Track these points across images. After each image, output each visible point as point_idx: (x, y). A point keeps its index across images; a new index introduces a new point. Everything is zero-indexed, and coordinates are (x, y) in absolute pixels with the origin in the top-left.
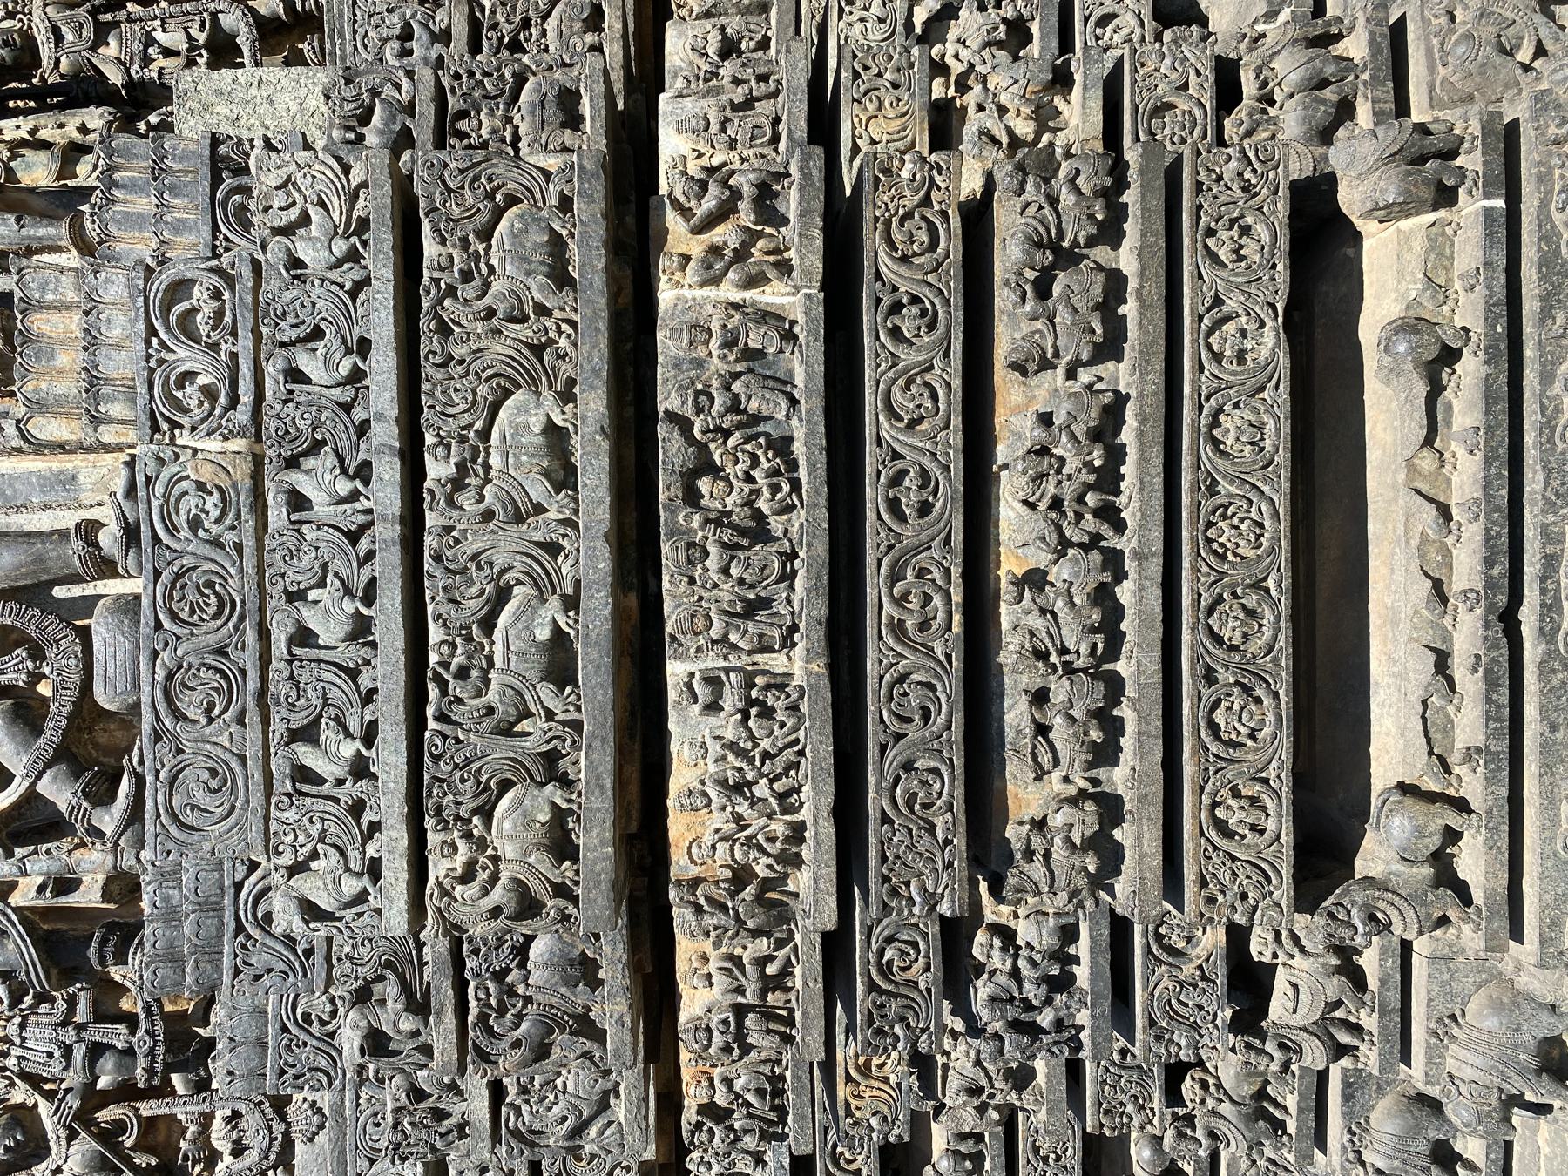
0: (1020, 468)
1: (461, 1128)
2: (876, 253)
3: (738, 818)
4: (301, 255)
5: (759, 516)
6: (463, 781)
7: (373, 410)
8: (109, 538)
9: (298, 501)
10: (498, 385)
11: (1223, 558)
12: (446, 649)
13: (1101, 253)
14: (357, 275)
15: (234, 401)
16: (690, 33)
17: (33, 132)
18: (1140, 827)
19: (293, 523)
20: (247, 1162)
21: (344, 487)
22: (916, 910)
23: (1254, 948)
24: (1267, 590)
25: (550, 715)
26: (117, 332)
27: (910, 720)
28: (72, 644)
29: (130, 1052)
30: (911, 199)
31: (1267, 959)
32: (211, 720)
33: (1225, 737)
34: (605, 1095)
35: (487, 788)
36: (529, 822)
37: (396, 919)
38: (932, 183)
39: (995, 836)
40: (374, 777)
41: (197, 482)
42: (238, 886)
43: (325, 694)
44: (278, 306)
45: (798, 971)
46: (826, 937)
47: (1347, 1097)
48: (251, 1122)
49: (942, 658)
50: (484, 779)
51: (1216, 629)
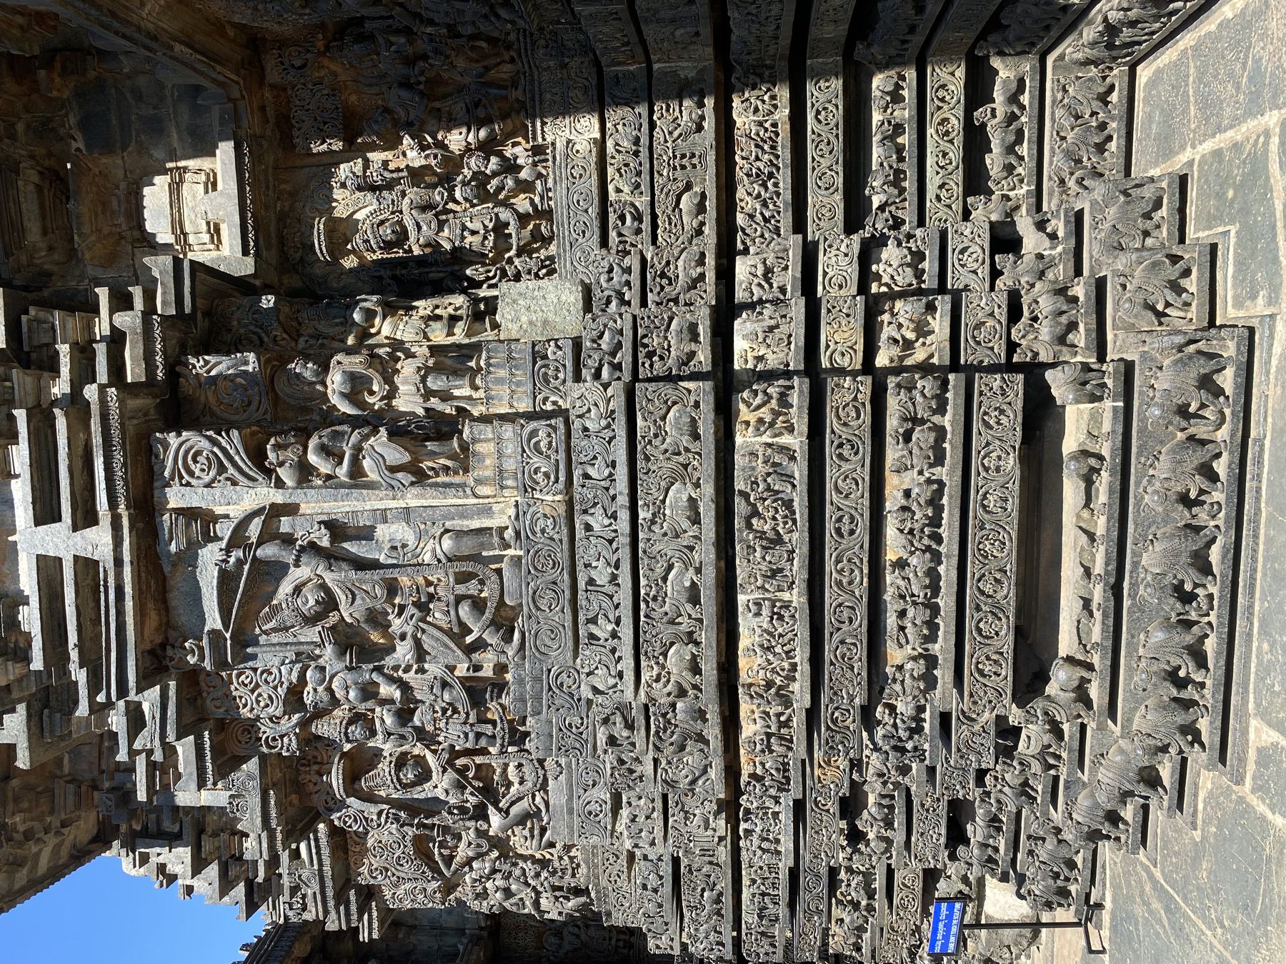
1: (641, 778)
3: (768, 660)
5: (778, 533)
9: (588, 527)
11: (986, 557)
13: (936, 419)
14: (611, 434)
15: (557, 481)
25: (690, 616)
28: (495, 578)
30: (849, 398)
34: (706, 766)
36: (683, 659)
37: (629, 694)
42: (549, 671)
47: (1066, 788)
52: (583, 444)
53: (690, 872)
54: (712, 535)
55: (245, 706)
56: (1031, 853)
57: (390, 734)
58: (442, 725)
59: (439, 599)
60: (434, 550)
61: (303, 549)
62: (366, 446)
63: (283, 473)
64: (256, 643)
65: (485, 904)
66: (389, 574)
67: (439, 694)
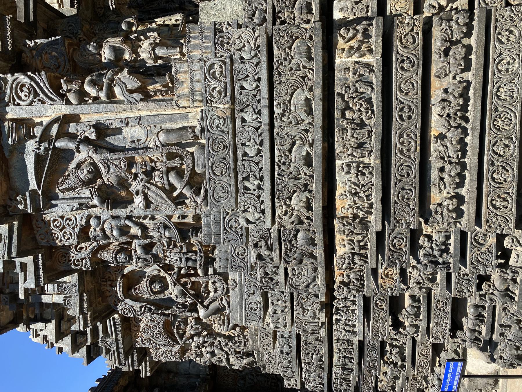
1: (277, 283)
3: (355, 201)
4: (243, 56)
5: (362, 120)
6: (284, 190)
8: (197, 130)
9: (244, 120)
11: (499, 130)
12: (280, 158)
13: (465, 41)
15: (226, 95)
17: (163, 22)
18: (469, 206)
20: (218, 294)
21: (255, 117)
22: (404, 227)
23: (505, 244)
24: (512, 139)
25: (306, 174)
26: (197, 78)
27: (404, 176)
28: (189, 156)
29: (195, 261)
30: (408, 29)
31: (509, 247)
32: (222, 175)
33: (497, 181)
34: (315, 277)
36: (300, 201)
37: (268, 223)
38: (414, 24)
39: (427, 208)
40: (262, 189)
42: (224, 218)
45: (369, 244)
46: (377, 233)
48: (219, 284)
49: (413, 159)
51: (495, 150)
52: (240, 67)
53: (306, 344)
54: (320, 121)
55: (57, 238)
56: (502, 335)
57: (139, 259)
58: (168, 254)
59: (158, 170)
60: (154, 141)
61: (81, 141)
62: (116, 78)
63: (71, 97)
64: (57, 198)
65: (202, 359)
66: (130, 155)
67: (162, 232)
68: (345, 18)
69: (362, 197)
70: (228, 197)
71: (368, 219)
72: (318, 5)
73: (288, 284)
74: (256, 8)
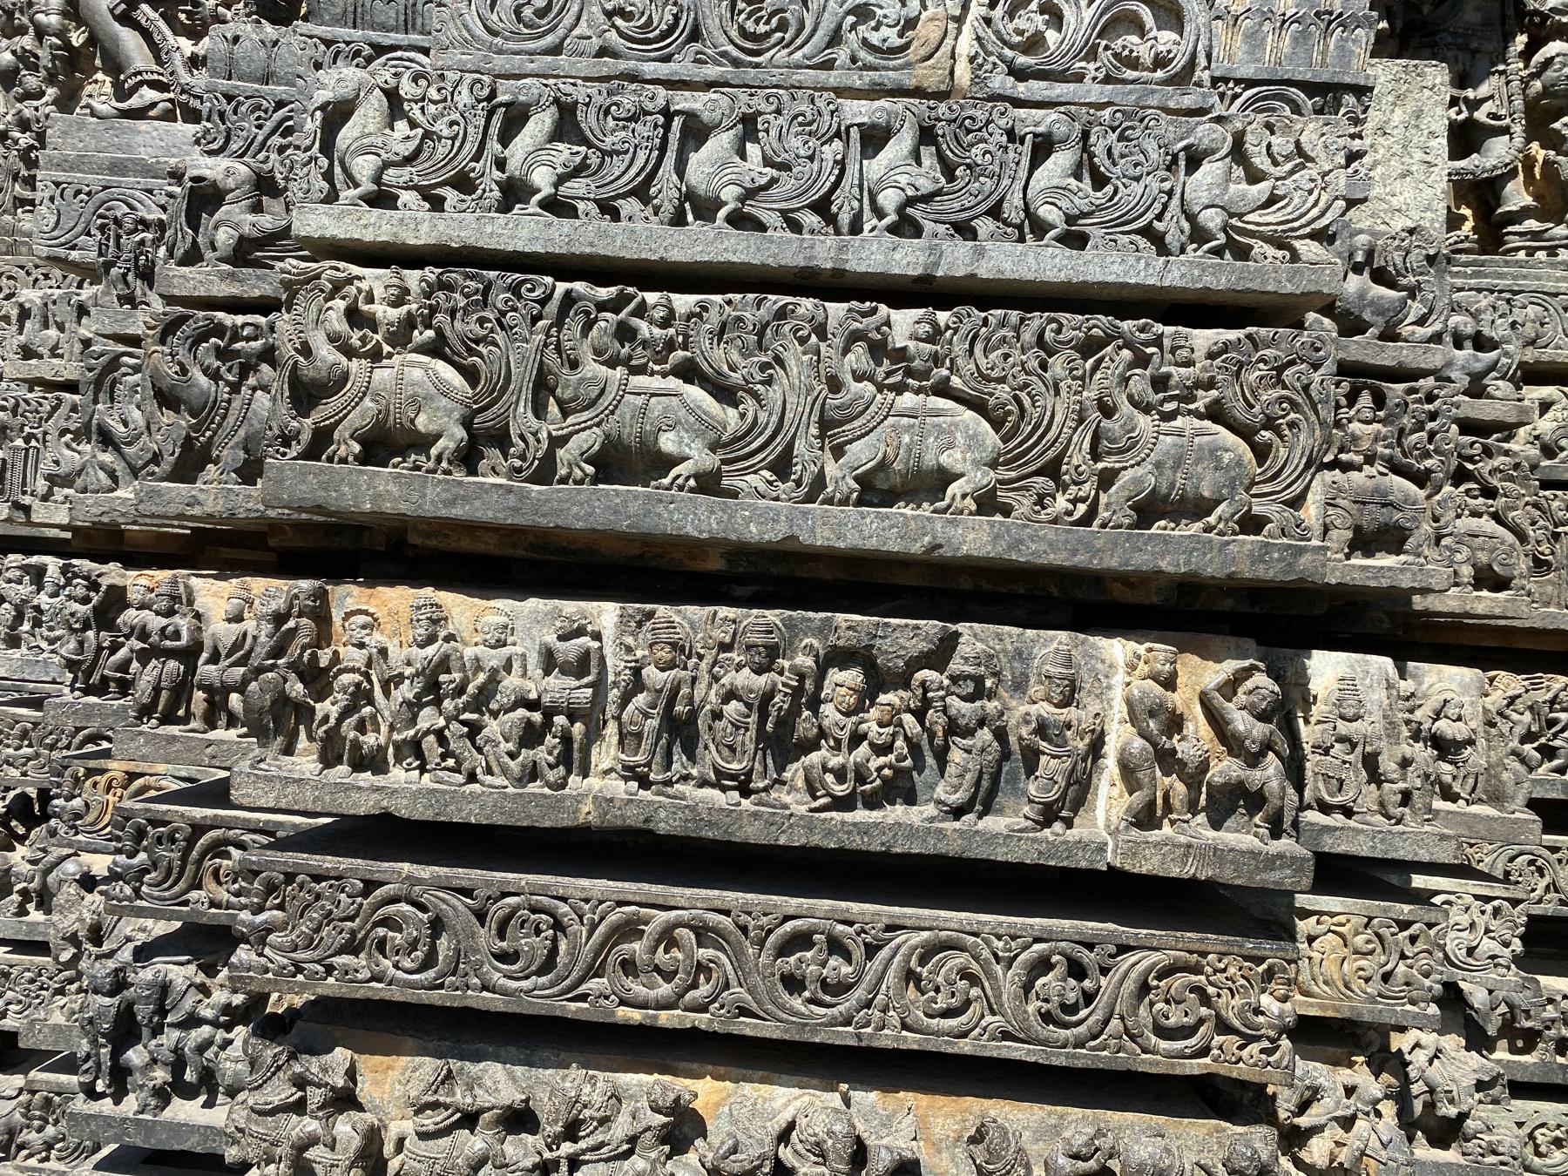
0: (837, 1128)
2: (1156, 949)
4: (1206, 167)
6: (482, 321)
7: (989, 245)
9: (874, 138)
10: (1009, 413)
12: (659, 314)
15: (1020, 74)
16: (1466, 699)
19: (848, 128)
25: (563, 440)
30: (1231, 1006)
32: (609, 15)
35: (469, 349)
36: (417, 404)
38: (1250, 1040)
40: (505, 207)
41: (917, 18)
43: (618, 153)
44: (1138, 132)
45: (232, 734)
50: (481, 348)
52: (1151, 146)
68: (1307, 701)
69: (413, 721)
70: (494, 33)
71: (303, 742)
72: (1385, 583)
73: (121, 348)
74: (1412, 292)
